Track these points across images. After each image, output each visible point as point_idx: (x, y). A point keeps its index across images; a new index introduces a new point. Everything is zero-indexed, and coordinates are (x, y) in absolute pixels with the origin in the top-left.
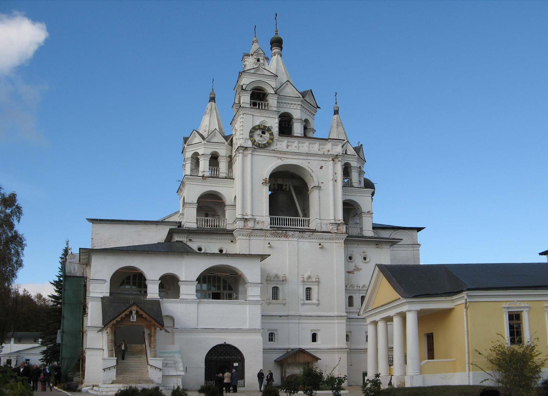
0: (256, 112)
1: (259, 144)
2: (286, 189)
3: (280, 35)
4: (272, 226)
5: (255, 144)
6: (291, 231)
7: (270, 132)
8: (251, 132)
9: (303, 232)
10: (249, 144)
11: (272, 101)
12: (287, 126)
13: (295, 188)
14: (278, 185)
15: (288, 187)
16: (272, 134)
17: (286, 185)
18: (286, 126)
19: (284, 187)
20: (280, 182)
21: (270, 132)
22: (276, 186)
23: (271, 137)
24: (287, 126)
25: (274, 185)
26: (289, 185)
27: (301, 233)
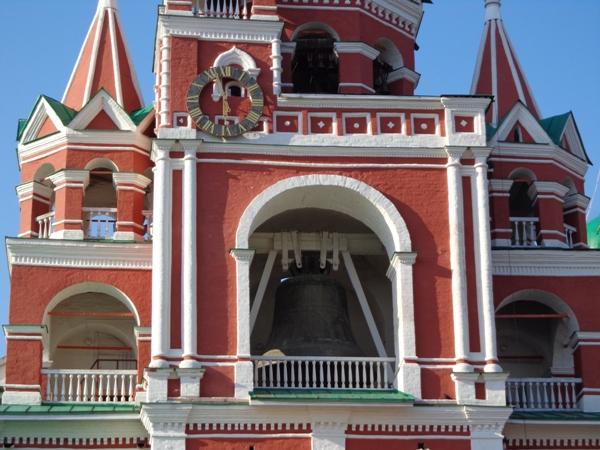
2: (329, 265)
12: (321, 65)
13: (360, 261)
14: (305, 254)
15: (335, 261)
17: (330, 255)
18: (312, 67)
19: (323, 259)
20: (310, 242)
22: (298, 260)
24: (321, 65)
25: (291, 254)
26: (334, 249)
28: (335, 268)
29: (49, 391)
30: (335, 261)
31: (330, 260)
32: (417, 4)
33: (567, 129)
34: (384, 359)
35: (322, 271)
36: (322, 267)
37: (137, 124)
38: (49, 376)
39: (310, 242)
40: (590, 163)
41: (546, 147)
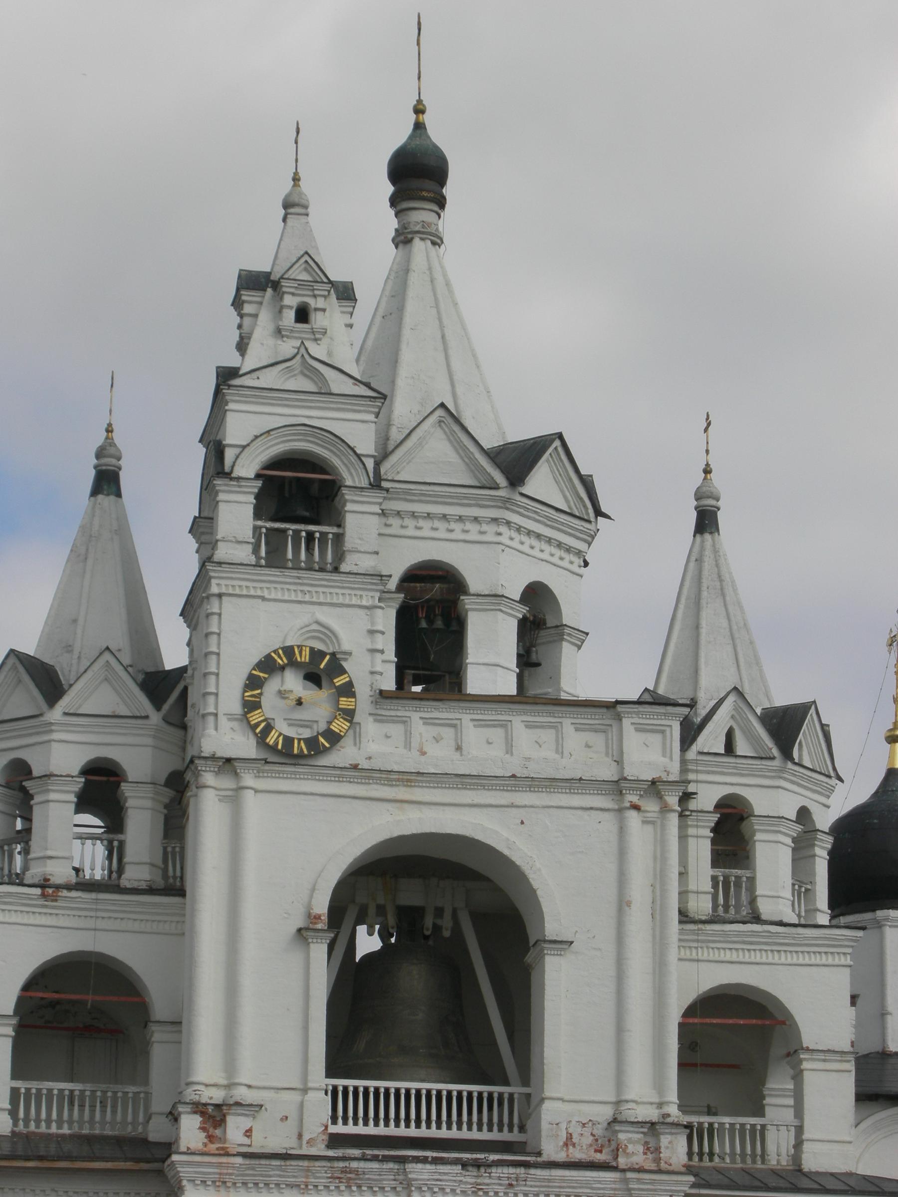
0: (278, 584)
1: (288, 741)
2: (437, 928)
3: (439, 134)
4: (339, 1128)
5: (271, 740)
6: (424, 1160)
7: (339, 681)
8: (253, 683)
9: (477, 1165)
10: (241, 745)
11: (360, 520)
15: (447, 923)
16: (348, 690)
17: (439, 912)
19: (429, 921)
20: (411, 894)
21: (339, 681)
23: (344, 702)
27: (473, 1171)
28: (447, 934)
29: (21, 1114)
30: (447, 923)
31: (439, 922)
32: (589, 522)
33: (808, 735)
34: (516, 1090)
35: (426, 938)
36: (427, 933)
37: (158, 708)
38: (23, 1091)
39: (411, 894)
40: (841, 780)
41: (769, 763)
